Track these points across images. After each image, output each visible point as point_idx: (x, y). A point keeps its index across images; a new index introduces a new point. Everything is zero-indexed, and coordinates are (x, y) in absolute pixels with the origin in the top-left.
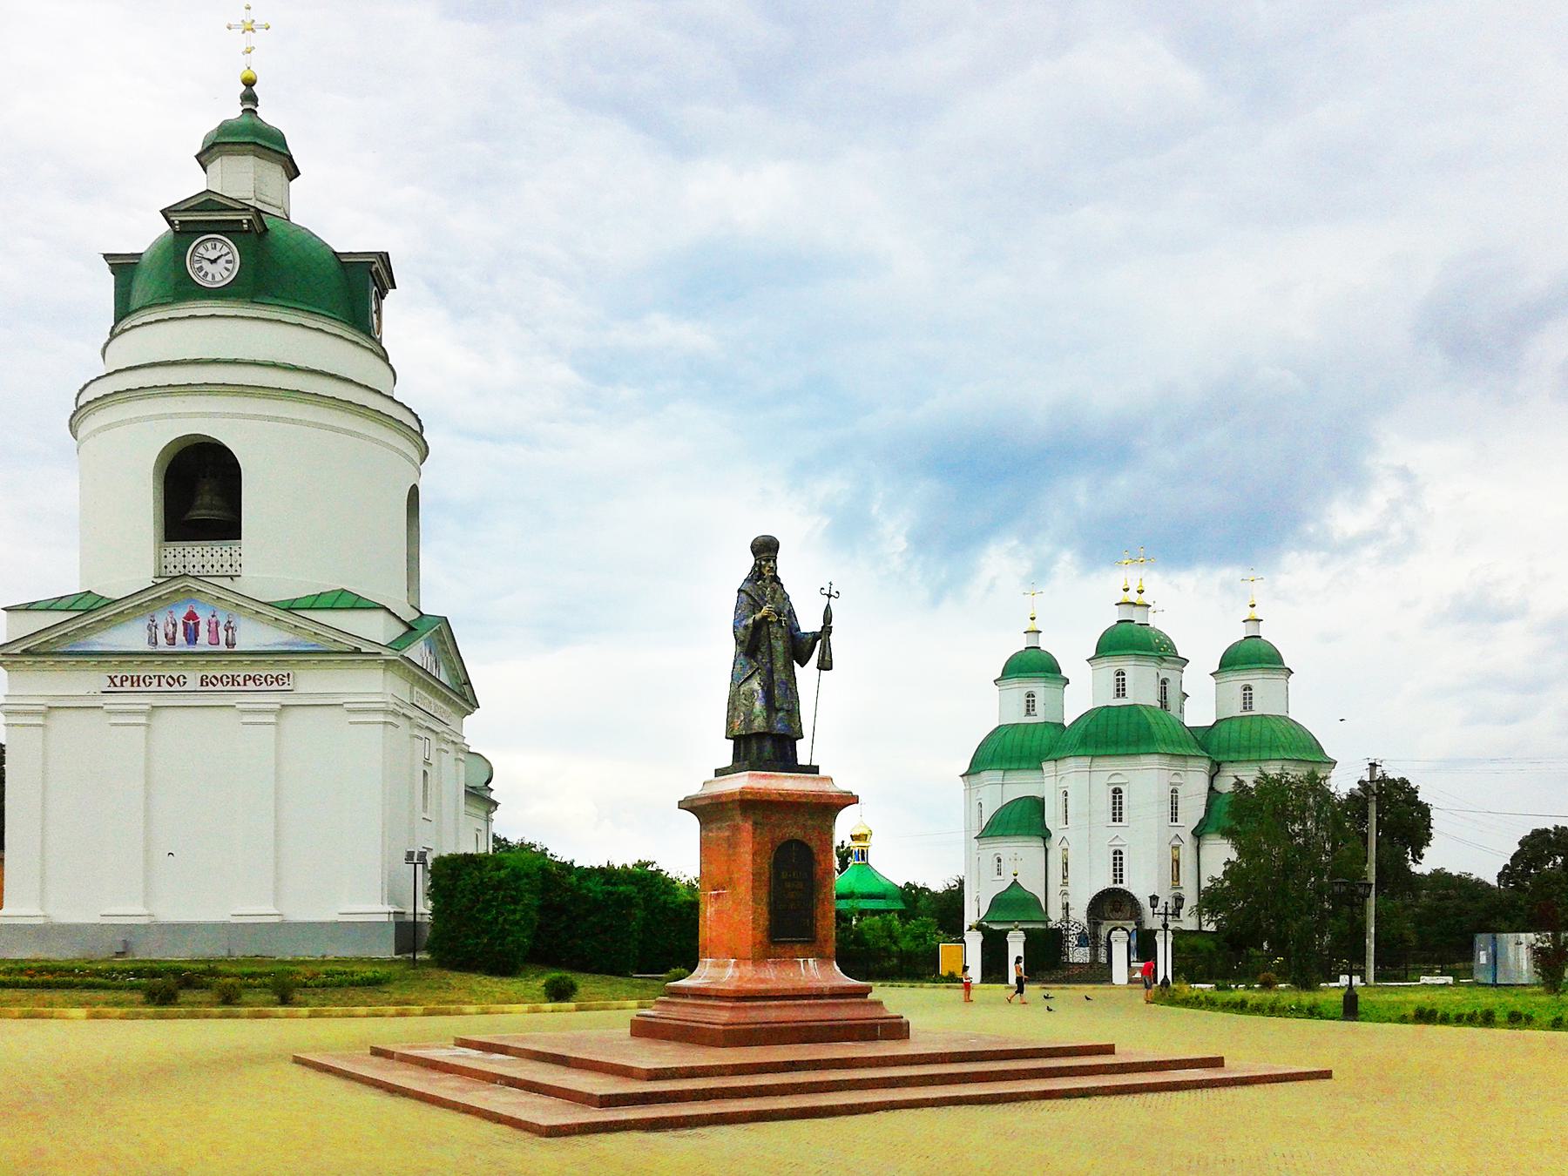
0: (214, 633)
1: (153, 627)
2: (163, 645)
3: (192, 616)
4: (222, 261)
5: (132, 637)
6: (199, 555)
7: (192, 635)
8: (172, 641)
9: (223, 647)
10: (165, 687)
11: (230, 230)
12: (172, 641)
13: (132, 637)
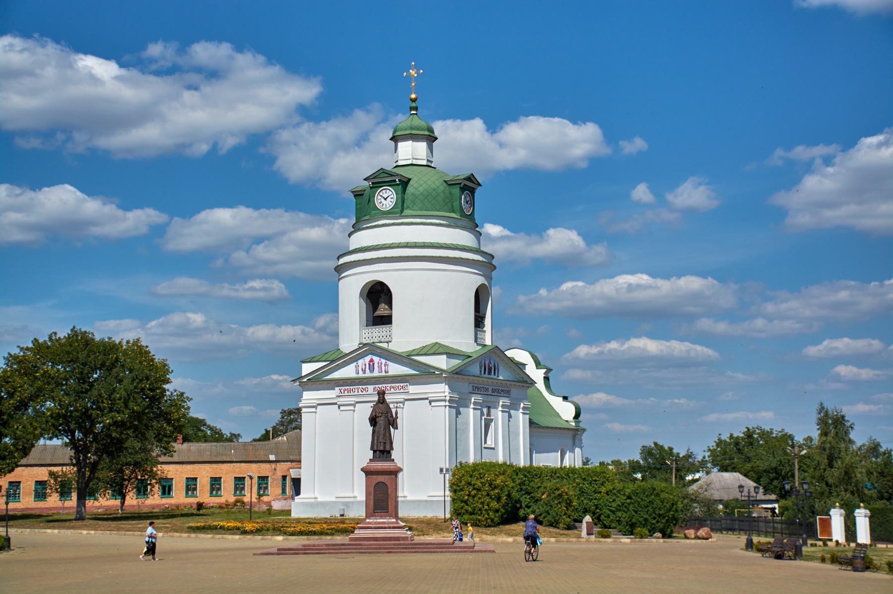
0: (380, 367)
1: (357, 367)
2: (361, 375)
3: (372, 360)
4: (389, 199)
5: (348, 372)
6: (376, 334)
7: (372, 369)
8: (364, 372)
9: (384, 374)
10: (360, 393)
11: (391, 183)
12: (364, 372)
13: (348, 372)
